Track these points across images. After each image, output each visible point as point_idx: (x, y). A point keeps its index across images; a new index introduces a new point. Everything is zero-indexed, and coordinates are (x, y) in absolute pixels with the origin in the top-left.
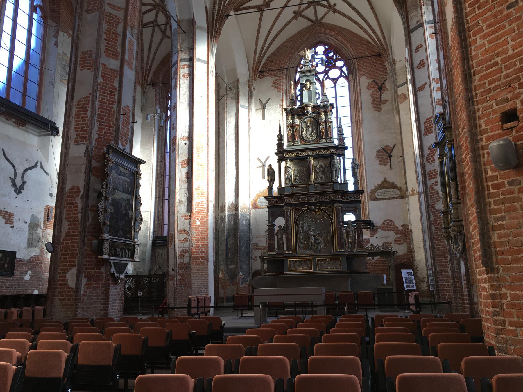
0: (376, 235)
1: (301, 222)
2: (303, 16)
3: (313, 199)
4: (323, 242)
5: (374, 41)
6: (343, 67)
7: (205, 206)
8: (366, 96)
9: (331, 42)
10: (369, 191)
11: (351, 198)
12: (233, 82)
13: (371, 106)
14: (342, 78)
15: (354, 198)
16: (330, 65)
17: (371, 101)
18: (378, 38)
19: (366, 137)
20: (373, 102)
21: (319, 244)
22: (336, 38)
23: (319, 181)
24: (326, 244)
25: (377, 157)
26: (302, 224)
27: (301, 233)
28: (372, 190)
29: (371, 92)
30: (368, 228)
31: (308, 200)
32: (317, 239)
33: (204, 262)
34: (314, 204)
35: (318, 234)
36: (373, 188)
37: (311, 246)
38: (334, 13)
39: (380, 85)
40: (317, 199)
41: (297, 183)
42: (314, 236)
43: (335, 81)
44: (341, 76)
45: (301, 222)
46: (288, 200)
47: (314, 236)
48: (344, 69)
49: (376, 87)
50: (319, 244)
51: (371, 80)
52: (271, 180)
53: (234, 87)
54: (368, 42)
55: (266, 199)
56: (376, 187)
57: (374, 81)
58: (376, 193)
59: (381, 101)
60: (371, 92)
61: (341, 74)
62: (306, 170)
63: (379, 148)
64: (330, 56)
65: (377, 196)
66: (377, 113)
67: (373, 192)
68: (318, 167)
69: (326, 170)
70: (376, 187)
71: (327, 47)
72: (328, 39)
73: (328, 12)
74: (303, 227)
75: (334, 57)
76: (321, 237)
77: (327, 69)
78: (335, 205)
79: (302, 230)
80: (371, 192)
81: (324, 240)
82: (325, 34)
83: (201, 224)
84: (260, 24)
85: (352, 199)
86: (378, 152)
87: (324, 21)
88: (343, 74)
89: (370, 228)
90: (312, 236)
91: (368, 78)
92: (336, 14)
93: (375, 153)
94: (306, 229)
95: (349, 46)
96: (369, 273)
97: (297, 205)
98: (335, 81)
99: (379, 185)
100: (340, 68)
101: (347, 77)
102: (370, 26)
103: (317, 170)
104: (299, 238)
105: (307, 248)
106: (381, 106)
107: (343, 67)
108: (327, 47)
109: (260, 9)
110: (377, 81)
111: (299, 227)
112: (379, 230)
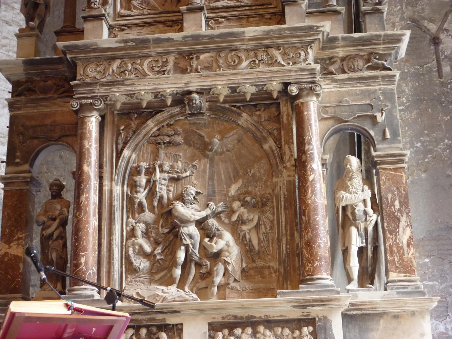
37: (185, 266)
42: (201, 224)
47: (200, 223)
94: (163, 190)
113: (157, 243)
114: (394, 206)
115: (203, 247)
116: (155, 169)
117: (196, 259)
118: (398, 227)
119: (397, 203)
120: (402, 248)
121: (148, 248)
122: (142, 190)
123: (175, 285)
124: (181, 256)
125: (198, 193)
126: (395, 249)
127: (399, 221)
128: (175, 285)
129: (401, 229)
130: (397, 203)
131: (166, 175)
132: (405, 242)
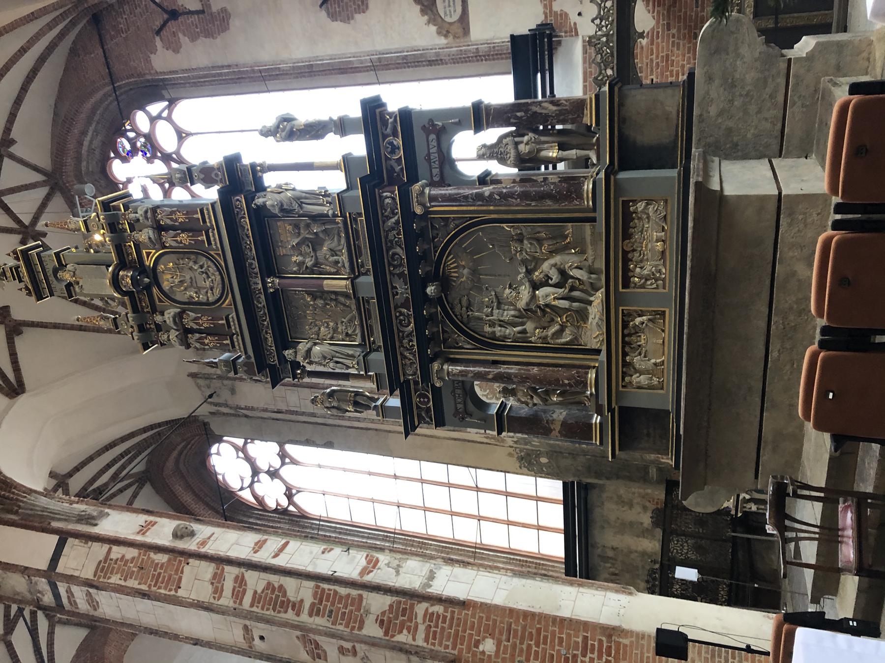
0: (573, 18)
1: (487, 329)
2: (36, 219)
3: (402, 290)
4: (557, 259)
5: (61, 36)
6: (148, 114)
7: (439, 609)
8: (197, 54)
9: (97, 143)
10: (443, 41)
11: (394, 149)
12: (199, 387)
13: (218, 40)
14: (174, 116)
15: (395, 134)
16: (151, 149)
17: (207, 40)
18: (50, 26)
19: (299, 51)
20: (209, 34)
21: (563, 273)
22: (84, 133)
23: (344, 258)
24: (567, 247)
25: (348, 19)
26: (492, 324)
27: (524, 332)
28: (439, 33)
29: (184, 40)
30: (550, 42)
31: (405, 305)
32: (548, 277)
33: (618, 644)
34: (418, 285)
35: (529, 272)
36: (433, 29)
37: (572, 299)
38: (13, 142)
39: (166, 16)
40: (401, 275)
41: (358, 331)
42: (535, 286)
43: (182, 135)
44: (169, 119)
45: (487, 329)
46: (411, 371)
47: (535, 286)
48: (155, 108)
49: (172, 26)
50: (563, 273)
51: (158, 39)
52: (359, 402)
53: (209, 387)
54: (73, 52)
55: (414, 428)
56: (429, 22)
57: (158, 33)
58: (448, 19)
59: (203, 12)
60: (184, 40)
61: (165, 119)
62: (314, 298)
63: (323, 14)
64: (128, 147)
65: (456, 17)
66: (235, 23)
67: (444, 30)
68: (300, 258)
69: (304, 234)
70: (429, 22)
71: (112, 155)
72: (91, 151)
73: (12, 157)
74: (503, 324)
75: (131, 135)
76: (538, 262)
77: (159, 154)
78: (418, 210)
79: (514, 325)
80: (446, 36)
81: (552, 253)
82: (78, 159)
83: (492, 636)
84: (56, 326)
85: (399, 142)
86: (333, 16)
87: (45, 162)
88: (165, 114)
89: (550, 37)
90: (533, 297)
91: (154, 51)
92: (13, 135)
93: (338, 25)
94: (508, 314)
95: (93, 100)
96: (691, 75)
97: (423, 342)
98: (182, 135)
99: (423, 12)
100: (153, 120)
101: (172, 102)
102: (23, 51)
103: (309, 262)
104: (544, 339)
105: (583, 315)
106: (215, 9)
107: (148, 114)
108: (112, 155)
109: (15, 329)
110: (158, 23)
111: (504, 338)
112: (556, 8)
113: (552, 320)
114: (522, 117)
115: (555, 286)
116: (490, 320)
117: (567, 290)
118: (541, 114)
119: (519, 114)
120: (560, 111)
121: (555, 328)
122: (508, 331)
123: (589, 307)
124: (564, 304)
125: (510, 287)
126: (561, 118)
127: (536, 112)
128: (589, 307)
129: (544, 111)
130: (519, 114)
131: (496, 312)
132: (554, 108)
